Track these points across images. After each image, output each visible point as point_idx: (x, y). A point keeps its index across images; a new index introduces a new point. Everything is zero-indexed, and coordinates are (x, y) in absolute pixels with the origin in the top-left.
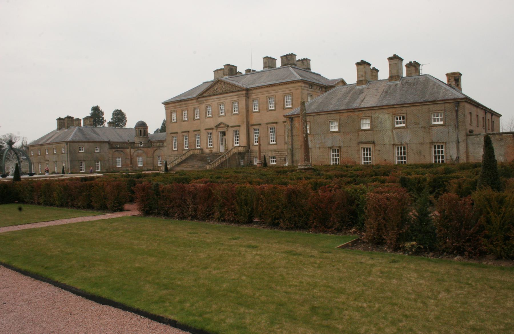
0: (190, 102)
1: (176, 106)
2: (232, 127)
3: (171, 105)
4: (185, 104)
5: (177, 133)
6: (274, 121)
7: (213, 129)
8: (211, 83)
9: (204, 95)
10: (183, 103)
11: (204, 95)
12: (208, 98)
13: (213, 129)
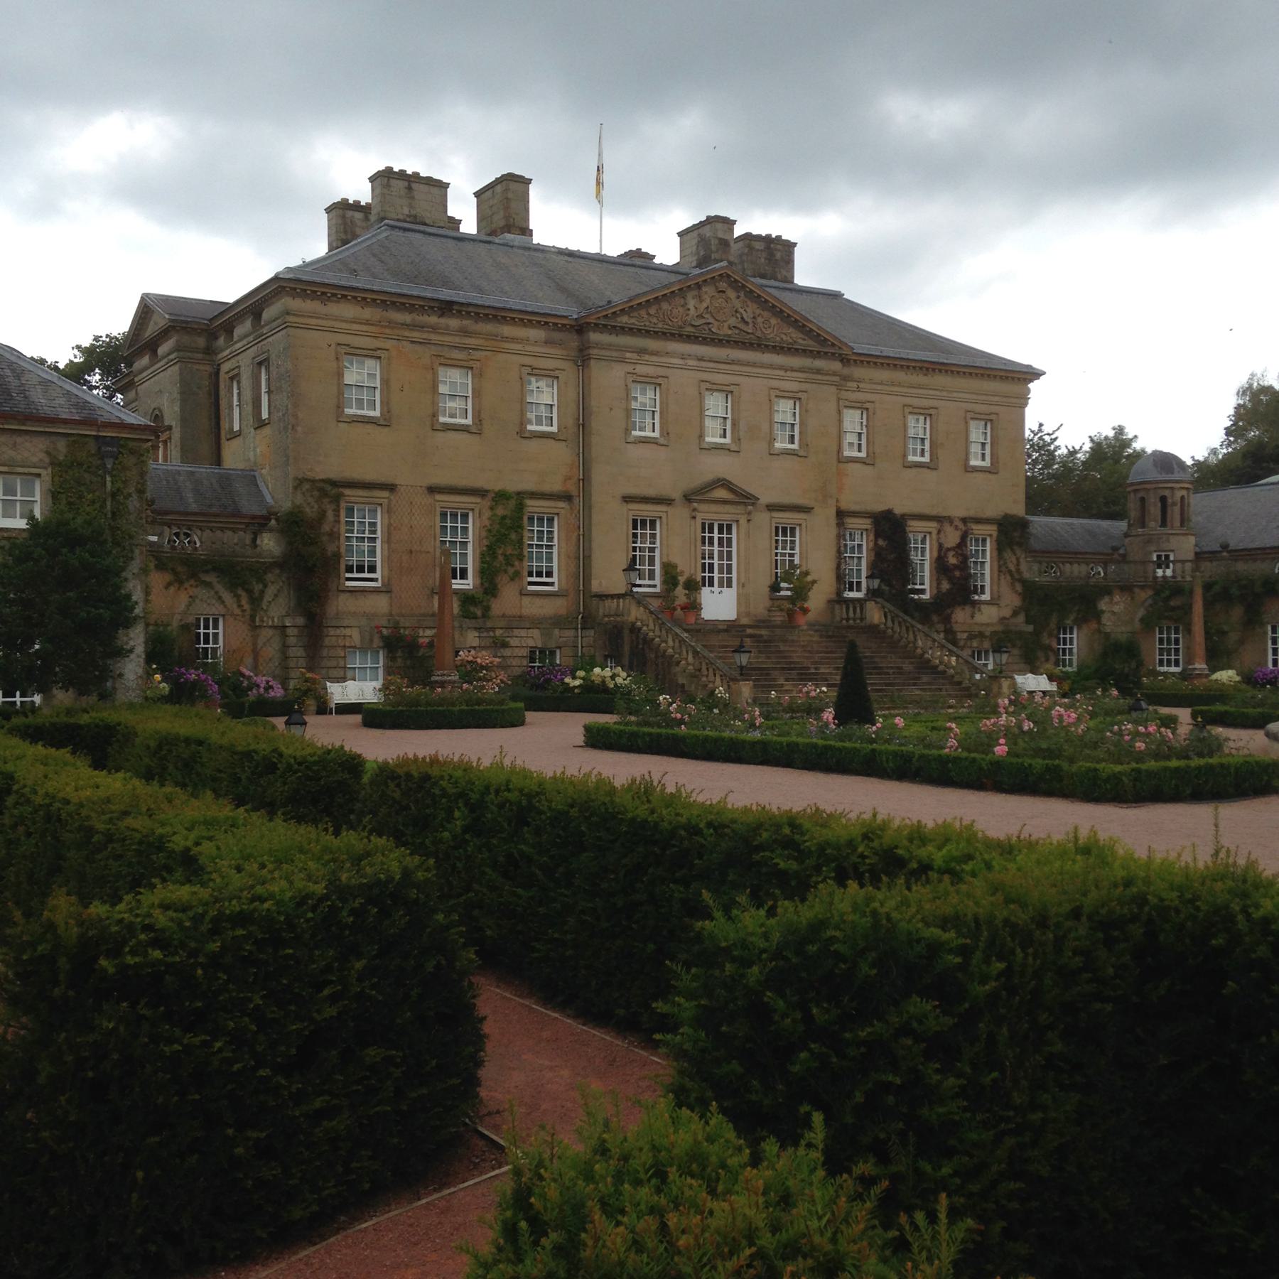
0: (507, 330)
1: (392, 324)
2: (771, 508)
3: (348, 310)
4: (464, 332)
5: (391, 488)
6: (927, 511)
7: (667, 501)
8: (673, 278)
9: (624, 319)
10: (454, 323)
11: (624, 319)
12: (651, 344)
13: (667, 501)
